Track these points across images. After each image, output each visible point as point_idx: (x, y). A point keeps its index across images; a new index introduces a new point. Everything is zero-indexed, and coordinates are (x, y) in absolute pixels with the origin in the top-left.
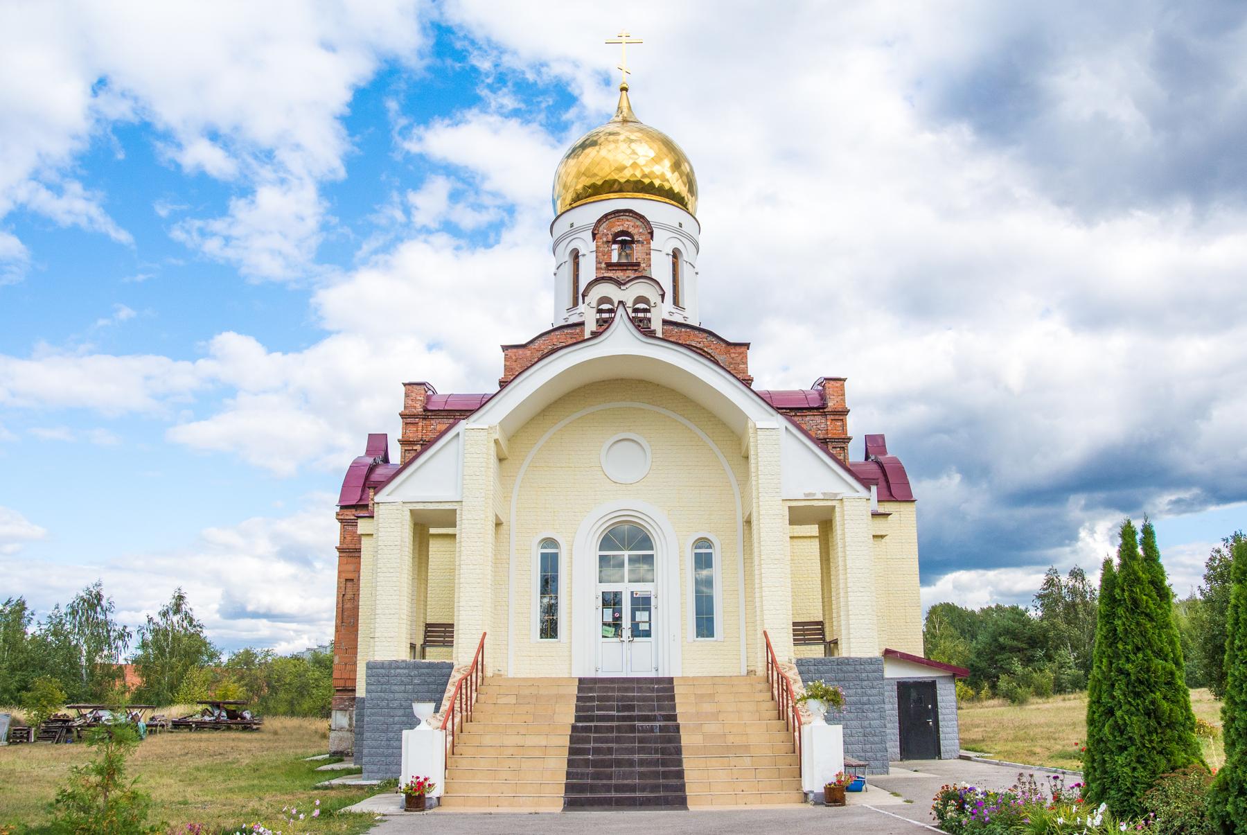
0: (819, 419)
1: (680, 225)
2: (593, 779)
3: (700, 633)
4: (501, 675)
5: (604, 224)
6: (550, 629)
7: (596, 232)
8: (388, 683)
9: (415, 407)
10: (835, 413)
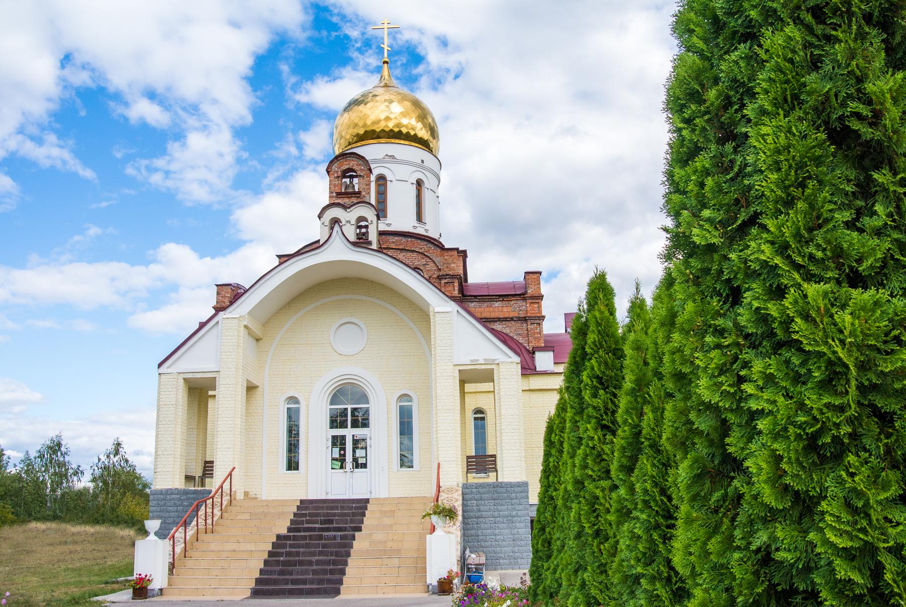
0: (520, 303)
1: (423, 161)
2: (279, 574)
3: (290, 468)
4: (257, 498)
5: (336, 164)
6: (293, 465)
7: (330, 170)
8: (165, 505)
9: (224, 302)
10: (533, 297)
